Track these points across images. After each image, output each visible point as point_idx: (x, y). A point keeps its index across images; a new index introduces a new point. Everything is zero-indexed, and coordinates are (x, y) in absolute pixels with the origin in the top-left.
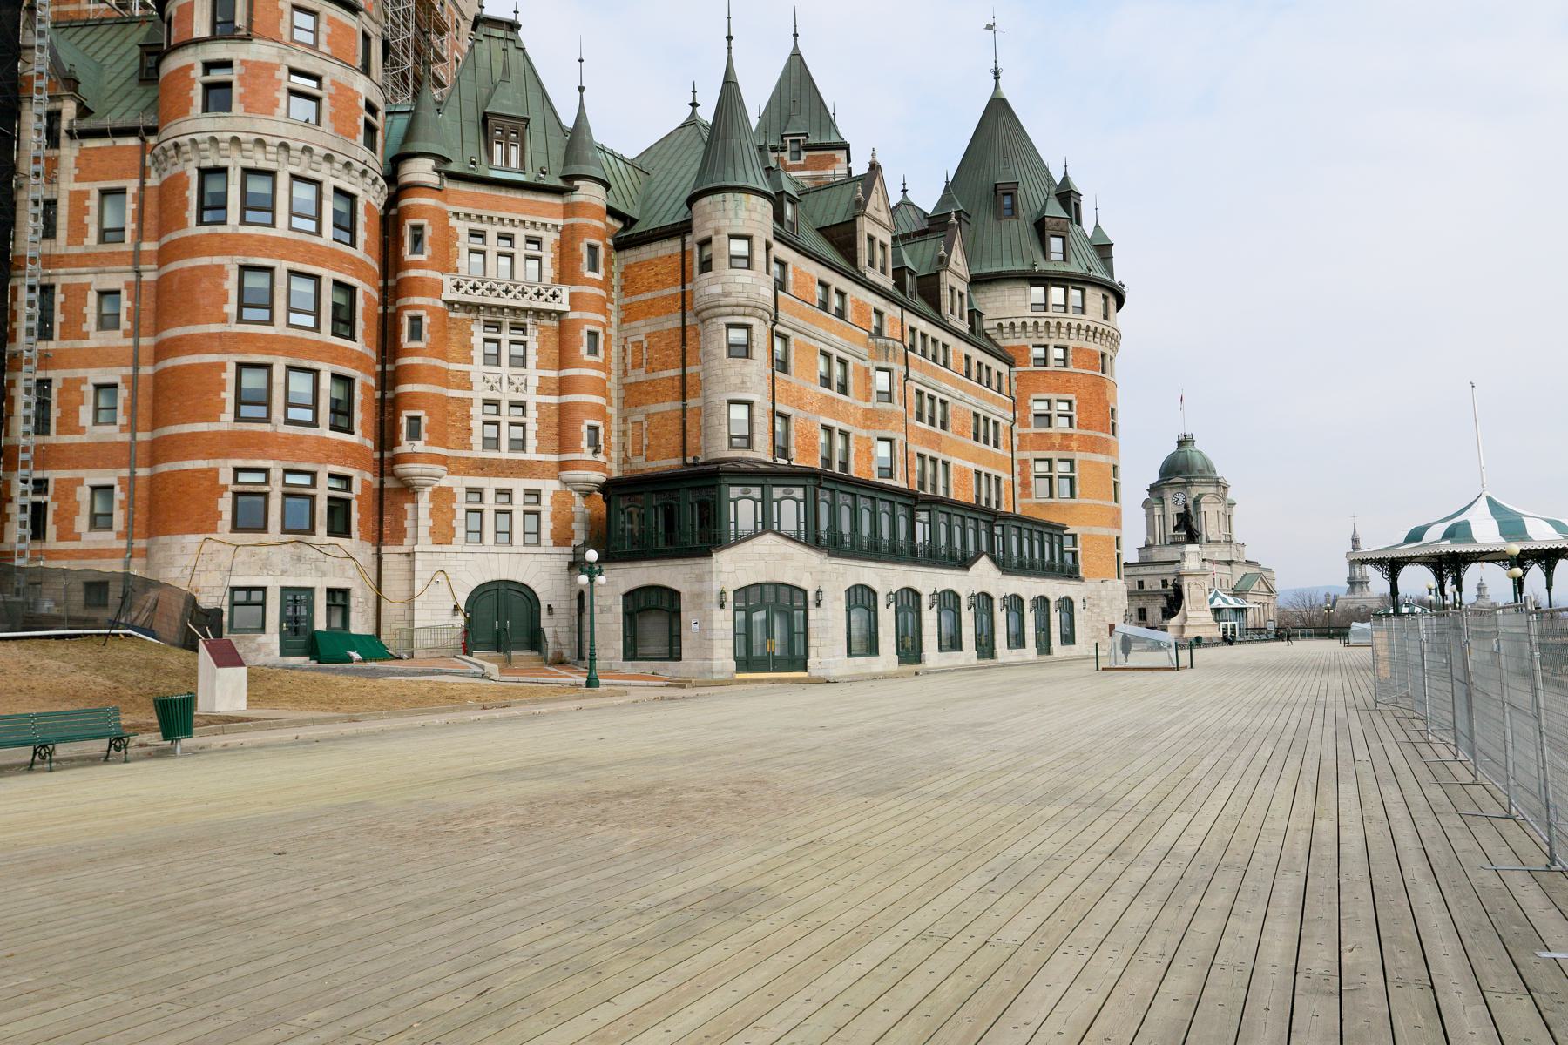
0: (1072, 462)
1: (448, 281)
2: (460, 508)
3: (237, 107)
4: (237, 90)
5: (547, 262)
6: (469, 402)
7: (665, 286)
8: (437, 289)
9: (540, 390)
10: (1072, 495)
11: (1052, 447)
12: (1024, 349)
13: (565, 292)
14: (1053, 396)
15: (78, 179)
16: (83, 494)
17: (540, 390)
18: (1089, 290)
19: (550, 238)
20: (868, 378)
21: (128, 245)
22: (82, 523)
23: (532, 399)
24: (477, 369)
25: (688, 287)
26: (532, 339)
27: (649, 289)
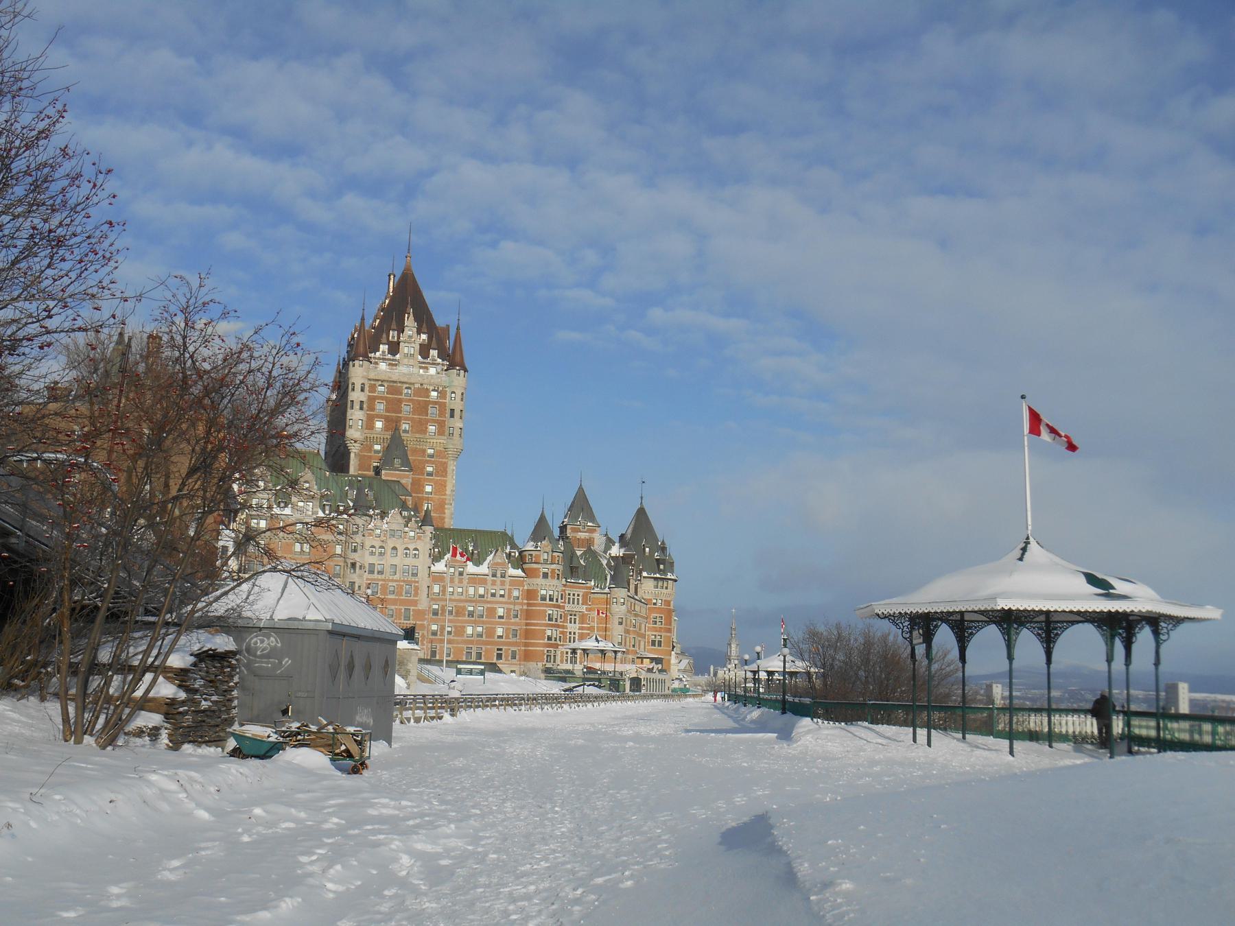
0: (661, 636)
1: (567, 605)
2: (565, 655)
3: (549, 578)
4: (550, 574)
5: (580, 600)
6: (567, 632)
7: (601, 605)
8: (563, 608)
9: (579, 629)
10: (661, 646)
11: (656, 631)
12: (651, 600)
13: (585, 607)
14: (658, 615)
15: (510, 586)
16: (510, 652)
17: (579, 629)
18: (669, 581)
19: (581, 594)
20: (631, 621)
21: (520, 600)
22: (510, 658)
23: (577, 631)
24: (569, 625)
25: (608, 606)
26: (577, 617)
27: (597, 604)
